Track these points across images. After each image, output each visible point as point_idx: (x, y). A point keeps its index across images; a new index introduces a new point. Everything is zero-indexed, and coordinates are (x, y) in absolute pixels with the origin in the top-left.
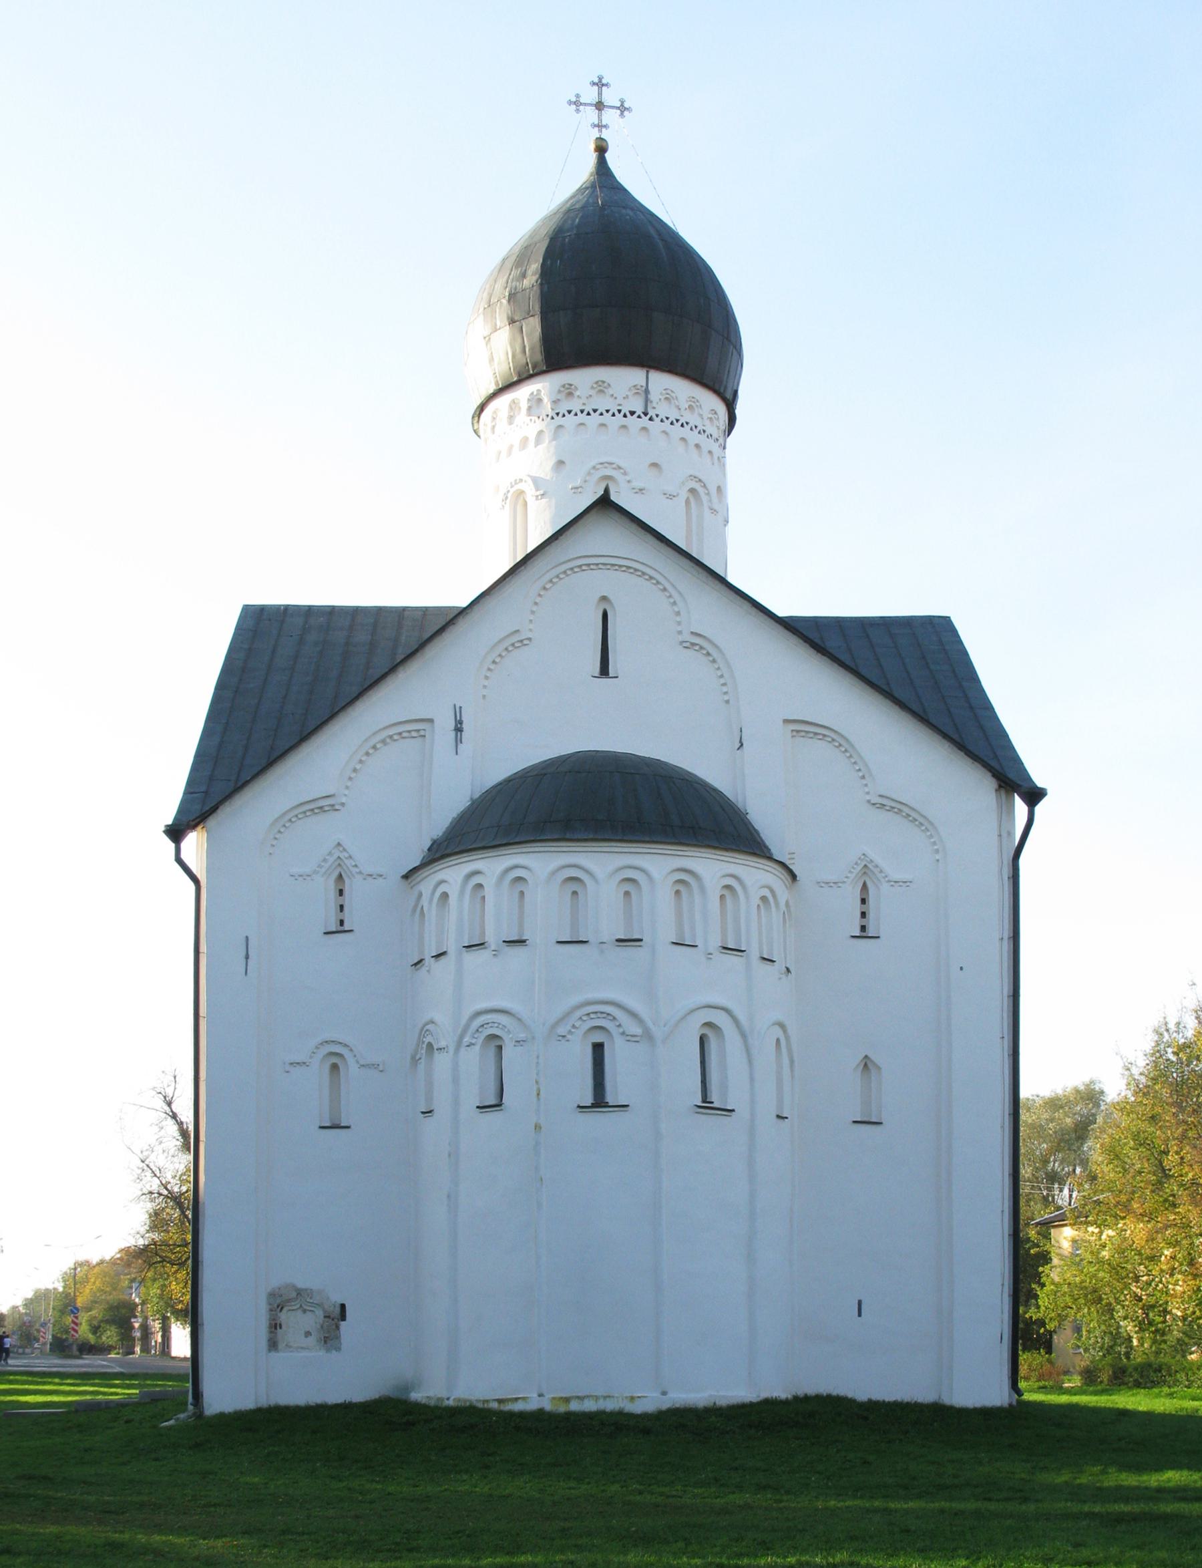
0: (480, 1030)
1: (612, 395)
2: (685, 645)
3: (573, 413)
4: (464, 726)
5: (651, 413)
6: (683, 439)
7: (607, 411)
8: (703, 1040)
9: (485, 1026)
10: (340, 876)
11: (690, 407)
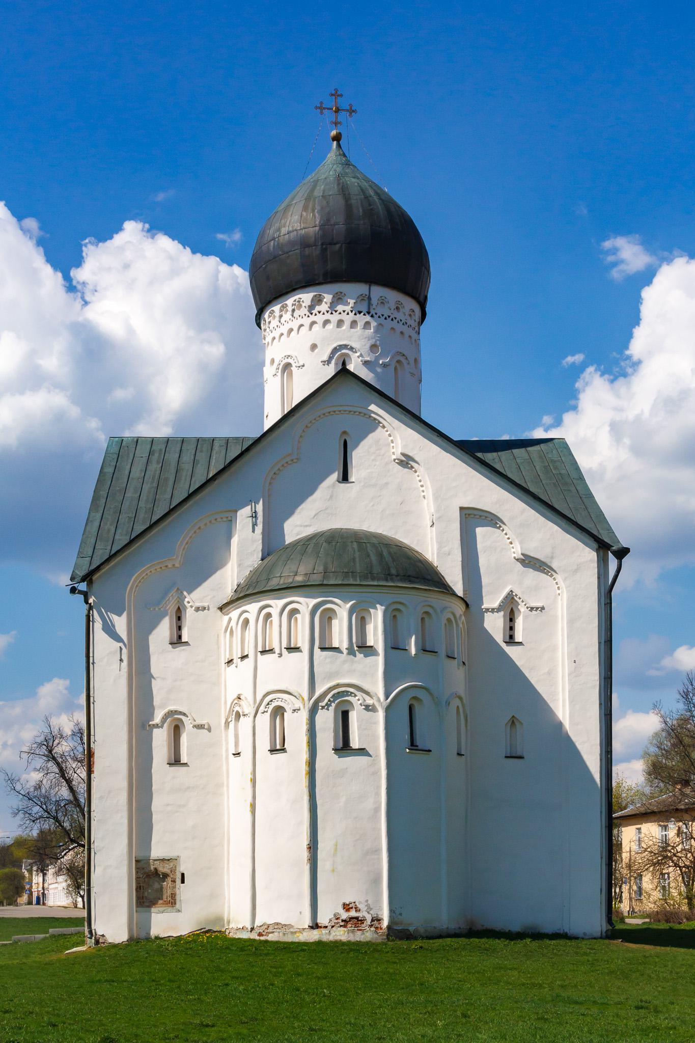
0: (270, 703)
2: (397, 461)
3: (321, 313)
5: (373, 312)
6: (393, 329)
8: (411, 708)
9: (273, 701)
10: (179, 608)
11: (397, 308)
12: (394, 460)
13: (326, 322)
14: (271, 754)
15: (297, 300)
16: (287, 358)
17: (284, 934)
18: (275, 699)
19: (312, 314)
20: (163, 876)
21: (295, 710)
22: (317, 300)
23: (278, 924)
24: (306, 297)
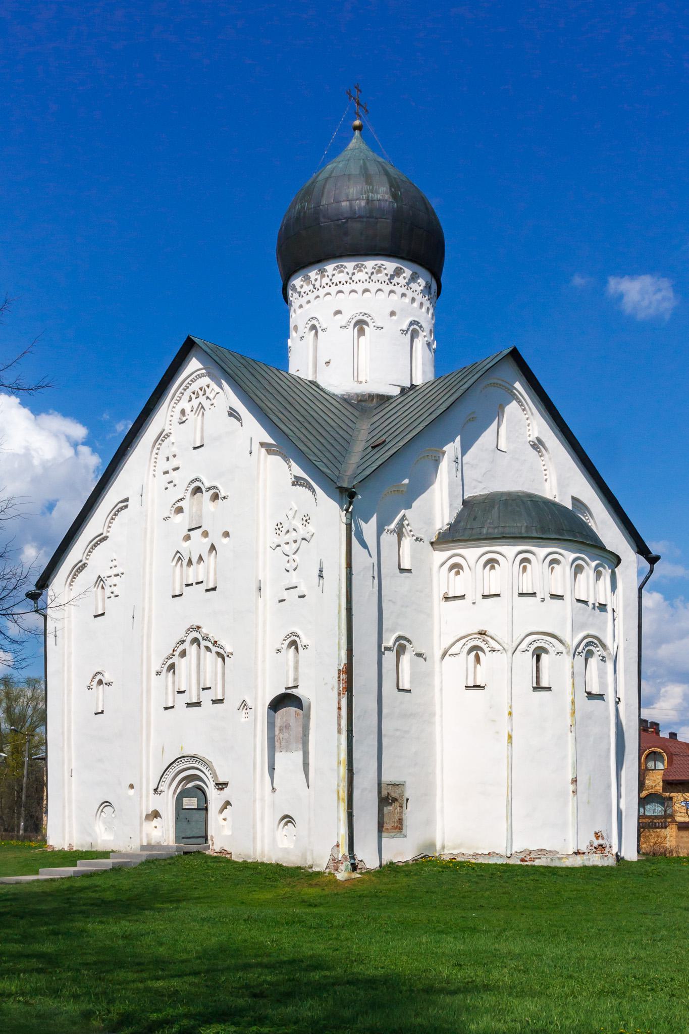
0: (533, 643)
2: (531, 443)
3: (400, 285)
9: (536, 641)
12: (530, 441)
13: (403, 295)
14: (533, 691)
15: (378, 266)
16: (363, 315)
17: (552, 860)
18: (538, 640)
19: (391, 283)
21: (558, 653)
22: (398, 272)
23: (541, 850)
24: (390, 266)
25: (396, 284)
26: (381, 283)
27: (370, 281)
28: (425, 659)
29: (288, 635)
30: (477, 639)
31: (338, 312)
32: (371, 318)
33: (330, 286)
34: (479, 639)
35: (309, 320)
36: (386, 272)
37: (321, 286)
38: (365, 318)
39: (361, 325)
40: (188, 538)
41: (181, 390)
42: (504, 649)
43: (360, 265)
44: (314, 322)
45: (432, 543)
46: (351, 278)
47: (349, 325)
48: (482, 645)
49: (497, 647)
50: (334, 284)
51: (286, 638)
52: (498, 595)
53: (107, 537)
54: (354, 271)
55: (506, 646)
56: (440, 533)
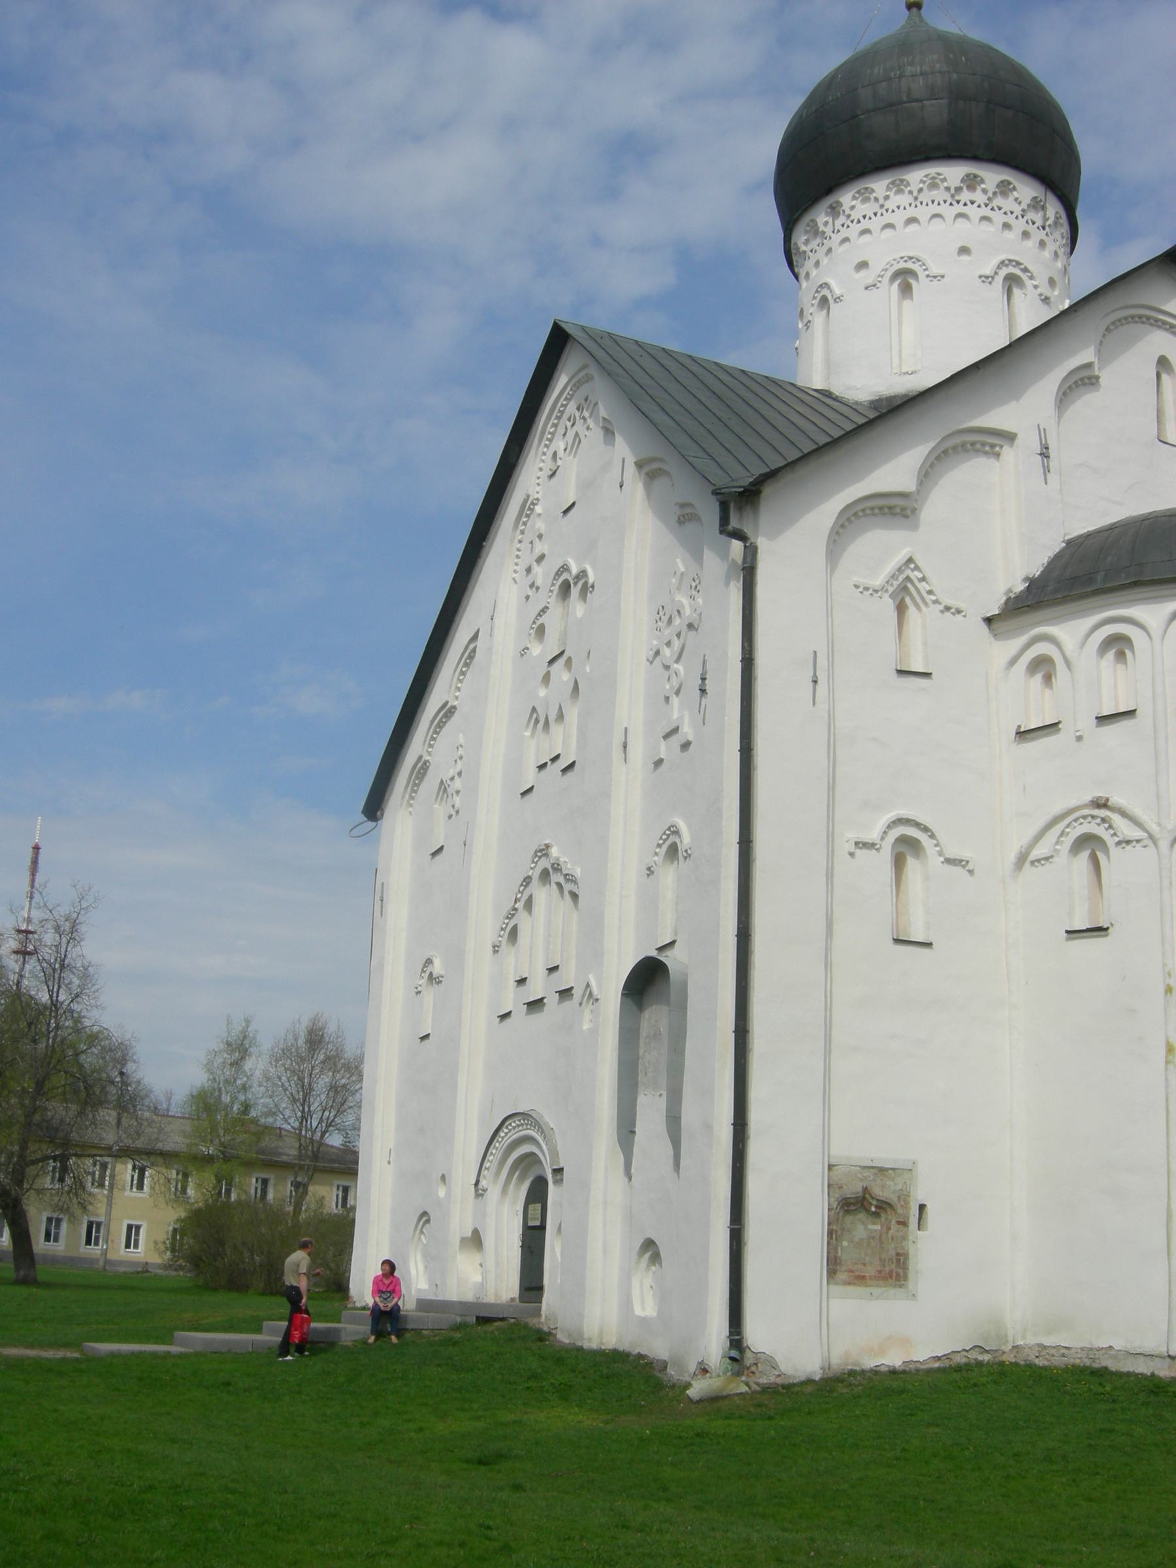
1: (1016, 199)
3: (976, 205)
4: (1050, 450)
7: (1012, 213)
19: (958, 202)
20: (877, 1207)
25: (969, 203)
26: (939, 204)
27: (918, 204)
28: (971, 872)
29: (664, 833)
30: (1090, 819)
31: (863, 265)
32: (920, 263)
33: (848, 227)
34: (1093, 817)
35: (817, 291)
36: (946, 184)
37: (833, 232)
38: (909, 265)
39: (904, 278)
40: (546, 678)
41: (553, 421)
42: (1151, 837)
43: (898, 182)
44: (825, 292)
45: (989, 621)
46: (882, 206)
47: (880, 282)
48: (1100, 831)
49: (1137, 833)
50: (855, 221)
51: (661, 842)
52: (1130, 713)
53: (454, 707)
54: (888, 193)
55: (1153, 828)
56: (1008, 599)
